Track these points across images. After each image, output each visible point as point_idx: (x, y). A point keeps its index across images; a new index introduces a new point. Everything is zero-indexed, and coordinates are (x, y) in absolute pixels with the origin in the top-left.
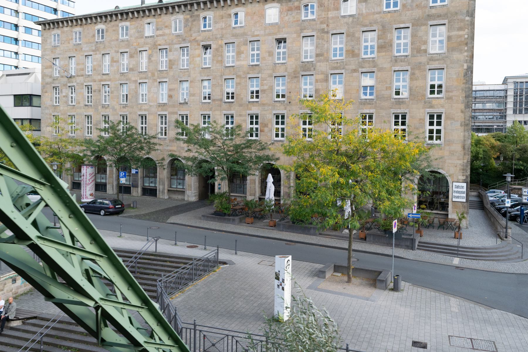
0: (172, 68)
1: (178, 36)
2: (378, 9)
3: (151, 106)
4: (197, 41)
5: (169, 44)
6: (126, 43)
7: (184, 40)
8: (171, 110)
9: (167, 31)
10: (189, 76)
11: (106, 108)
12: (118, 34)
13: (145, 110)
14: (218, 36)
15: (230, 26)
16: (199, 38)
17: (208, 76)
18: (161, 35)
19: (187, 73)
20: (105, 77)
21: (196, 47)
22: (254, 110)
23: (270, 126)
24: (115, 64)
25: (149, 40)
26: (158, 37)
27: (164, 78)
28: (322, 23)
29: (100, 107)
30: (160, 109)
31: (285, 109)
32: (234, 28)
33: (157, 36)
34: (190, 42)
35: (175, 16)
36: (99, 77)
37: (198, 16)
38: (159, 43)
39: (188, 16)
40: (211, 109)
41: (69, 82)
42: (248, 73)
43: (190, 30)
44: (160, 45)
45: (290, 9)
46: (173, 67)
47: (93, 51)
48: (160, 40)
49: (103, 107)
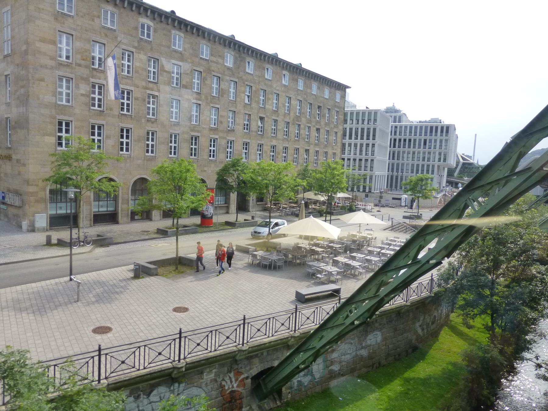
0: (223, 97)
1: (229, 68)
2: (323, 96)
3: (203, 128)
4: (243, 79)
5: (221, 74)
6: (180, 55)
7: (234, 75)
8: (221, 134)
9: (220, 60)
10: (236, 108)
11: (153, 123)
12: (170, 41)
13: (198, 131)
14: (257, 82)
15: (264, 76)
16: (244, 77)
17: (249, 111)
18: (214, 62)
19: (235, 105)
20: (151, 85)
21: (242, 84)
22: (274, 143)
23: (281, 154)
24: (165, 73)
25: (204, 63)
26: (213, 64)
27: (216, 104)
28: (305, 94)
29: (143, 120)
30: (212, 132)
31: (288, 144)
32: (266, 79)
33: (211, 61)
34: (238, 78)
35: (227, 50)
36: (144, 84)
37: (245, 58)
38: (212, 68)
39: (237, 55)
40: (250, 139)
41: (93, 77)
42: (272, 116)
43: (239, 68)
44: (213, 71)
45: (293, 79)
46: (225, 96)
47: (135, 48)
48: (214, 67)
49: (149, 120)
